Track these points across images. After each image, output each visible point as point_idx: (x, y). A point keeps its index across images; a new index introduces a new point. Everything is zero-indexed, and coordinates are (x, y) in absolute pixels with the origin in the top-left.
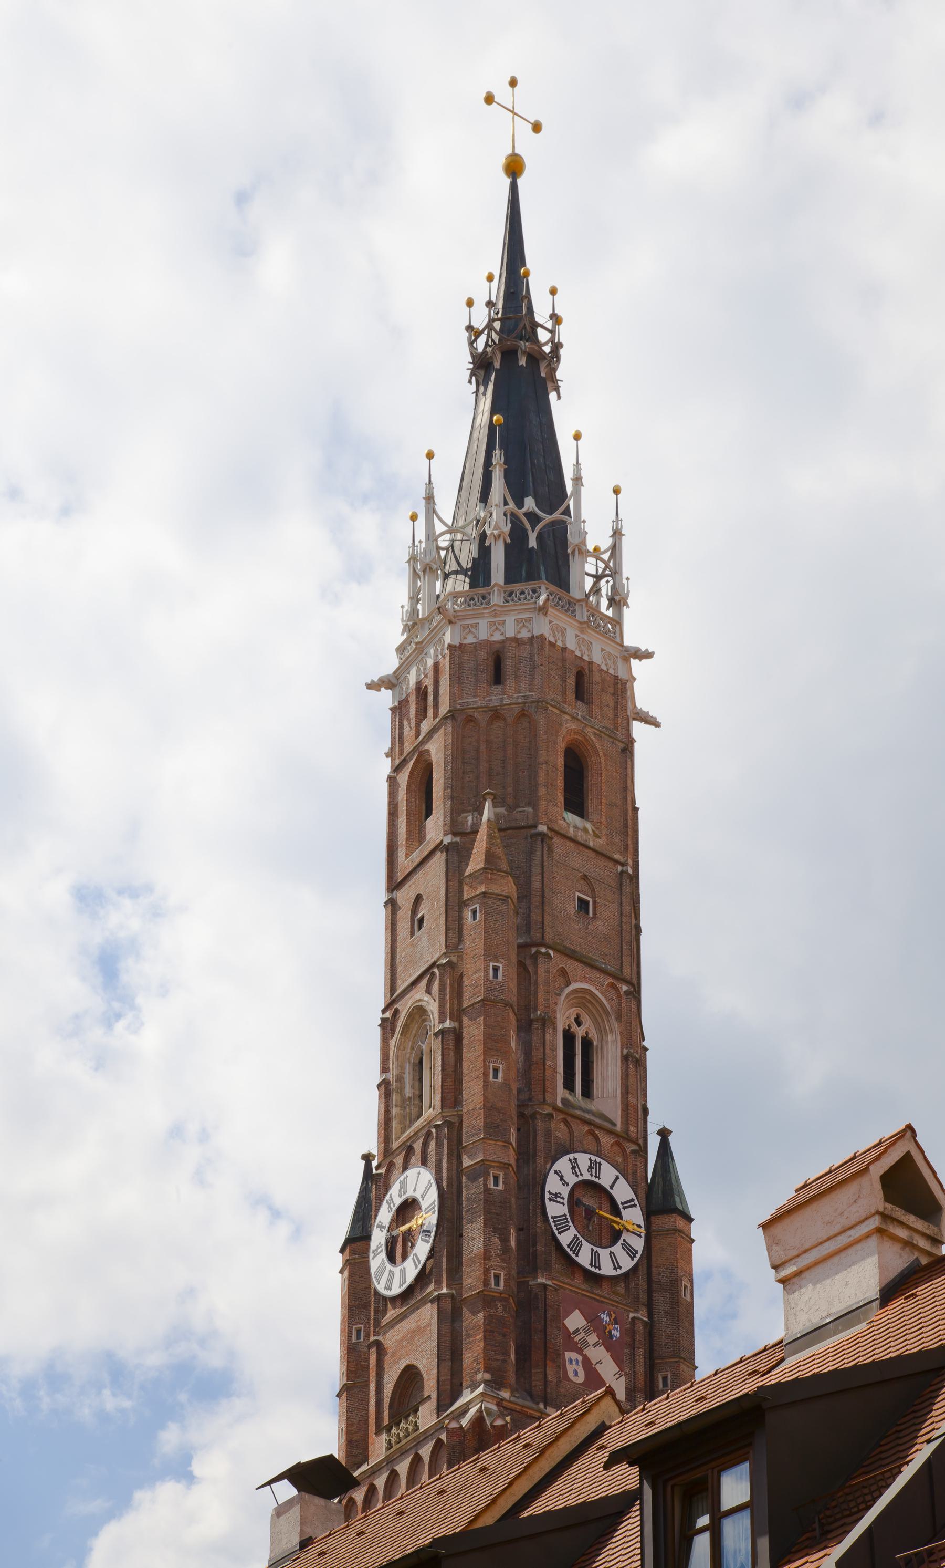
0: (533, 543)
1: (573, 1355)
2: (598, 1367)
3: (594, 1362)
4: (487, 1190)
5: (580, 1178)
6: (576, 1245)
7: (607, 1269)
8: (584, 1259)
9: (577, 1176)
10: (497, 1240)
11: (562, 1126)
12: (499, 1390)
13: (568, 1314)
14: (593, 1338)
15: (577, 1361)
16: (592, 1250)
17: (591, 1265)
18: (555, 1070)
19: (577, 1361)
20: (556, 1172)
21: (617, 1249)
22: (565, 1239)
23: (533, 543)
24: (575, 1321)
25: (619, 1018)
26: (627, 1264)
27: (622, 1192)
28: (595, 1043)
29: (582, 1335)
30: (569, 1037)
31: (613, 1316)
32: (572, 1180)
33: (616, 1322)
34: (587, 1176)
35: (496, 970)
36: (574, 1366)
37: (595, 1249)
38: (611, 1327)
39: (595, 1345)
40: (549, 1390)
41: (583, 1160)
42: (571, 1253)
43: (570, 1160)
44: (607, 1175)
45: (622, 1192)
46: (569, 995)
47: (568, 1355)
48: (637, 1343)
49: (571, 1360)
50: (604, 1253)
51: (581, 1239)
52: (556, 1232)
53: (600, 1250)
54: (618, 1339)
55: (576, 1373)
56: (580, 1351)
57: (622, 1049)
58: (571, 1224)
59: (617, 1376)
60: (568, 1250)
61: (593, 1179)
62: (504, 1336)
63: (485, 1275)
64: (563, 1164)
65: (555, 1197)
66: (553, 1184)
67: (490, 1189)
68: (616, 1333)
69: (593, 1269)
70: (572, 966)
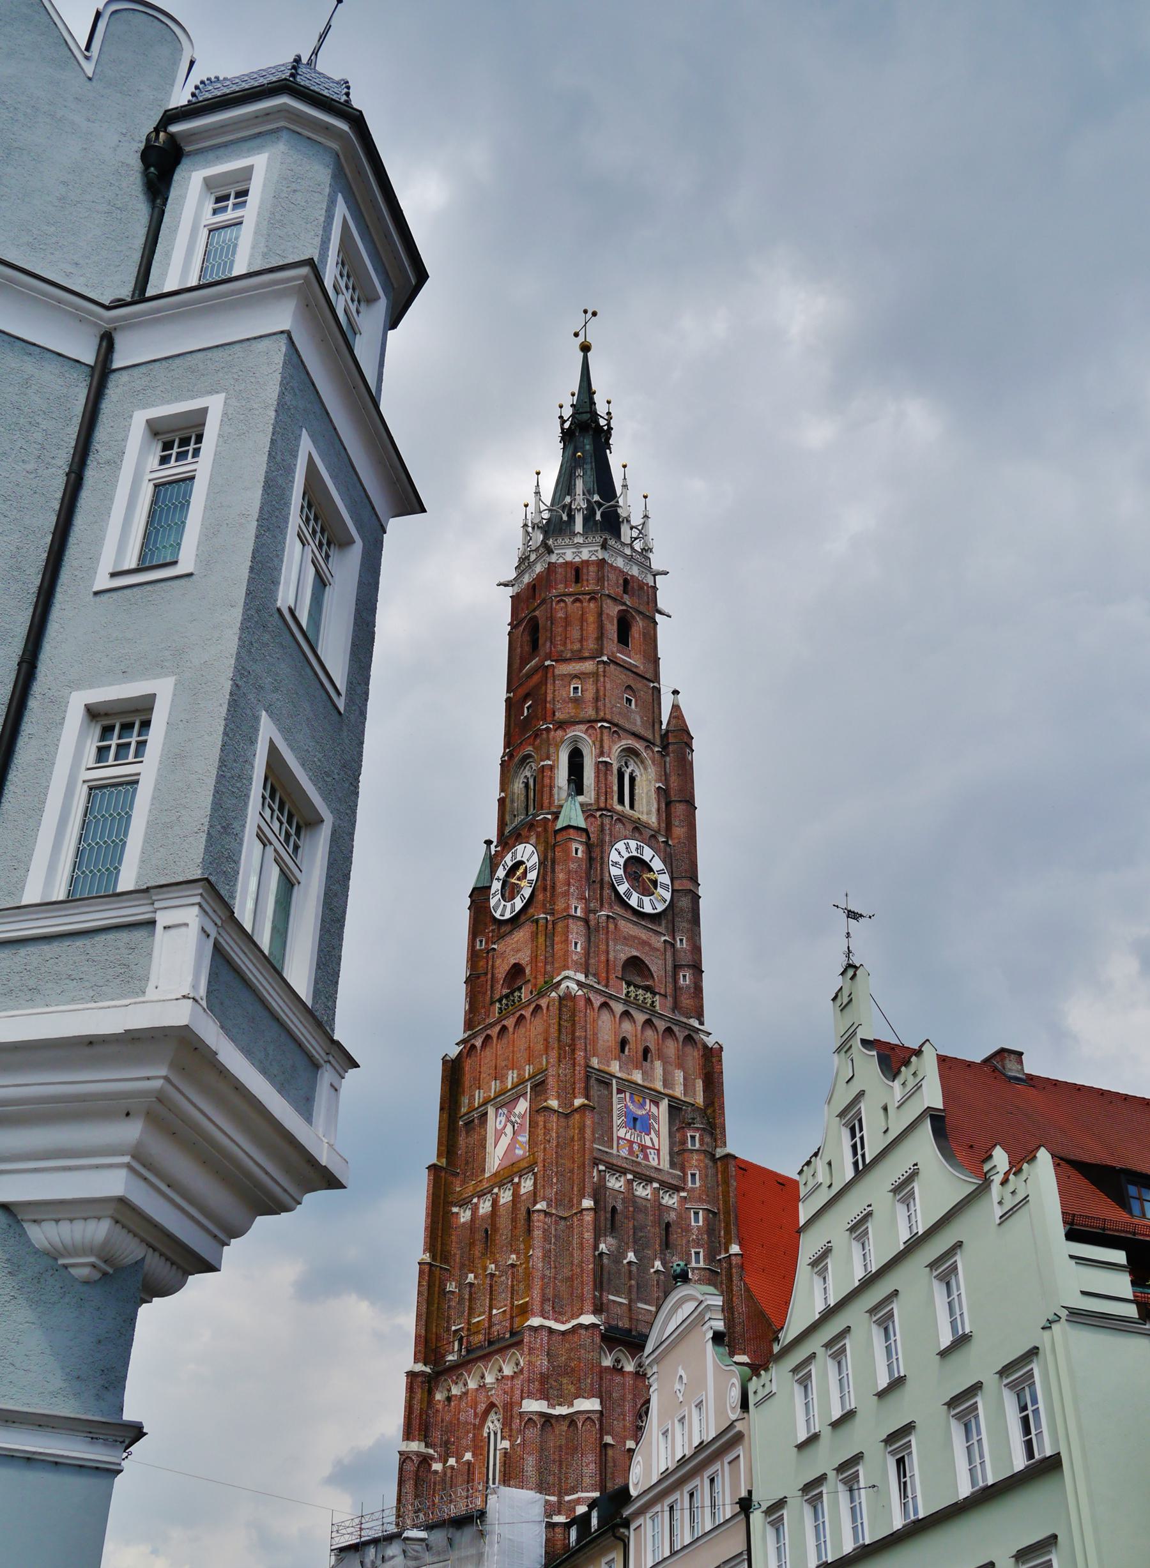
0: (598, 517)
6: (628, 893)
7: (648, 909)
8: (633, 902)
22: (622, 889)
23: (598, 517)
26: (660, 908)
27: (657, 864)
32: (626, 855)
34: (635, 854)
41: (633, 844)
44: (648, 854)
45: (657, 864)
50: (646, 900)
64: (620, 845)
65: (615, 864)
66: (614, 856)
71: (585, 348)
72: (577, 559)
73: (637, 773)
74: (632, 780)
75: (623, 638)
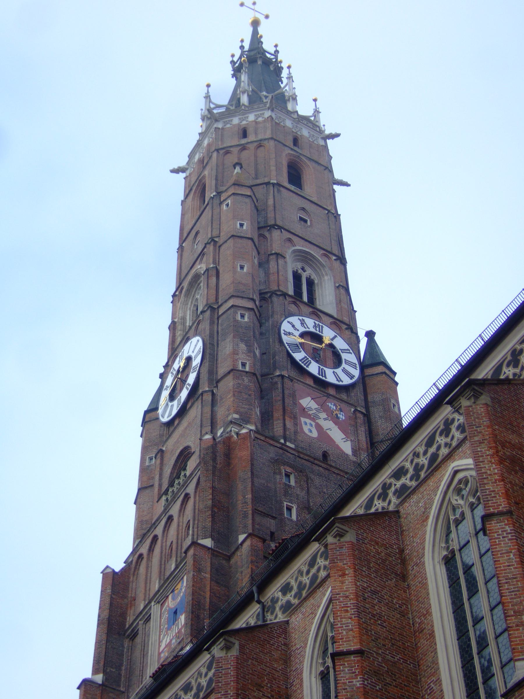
1: (308, 421)
2: (328, 431)
3: (325, 428)
4: (236, 321)
5: (307, 330)
7: (330, 378)
9: (305, 327)
10: (244, 346)
11: (293, 306)
12: (246, 424)
13: (302, 398)
14: (323, 415)
15: (311, 425)
16: (319, 367)
17: (319, 374)
18: (286, 279)
19: (311, 425)
20: (288, 322)
21: (339, 371)
24: (307, 402)
25: (331, 269)
28: (316, 282)
29: (314, 411)
30: (297, 277)
31: (339, 407)
33: (341, 410)
34: (312, 330)
35: (242, 225)
36: (309, 427)
37: (322, 367)
38: (337, 412)
39: (325, 419)
40: (287, 433)
42: (303, 365)
43: (300, 320)
46: (294, 251)
47: (303, 420)
48: (358, 424)
49: (306, 424)
51: (310, 359)
52: (291, 352)
53: (325, 368)
54: (343, 420)
55: (311, 431)
56: (313, 420)
57: (335, 283)
58: (301, 350)
59: (345, 440)
60: (300, 363)
61: (318, 332)
62: (250, 395)
63: (233, 361)
67: (238, 321)
68: (342, 417)
69: (321, 377)
70: (295, 239)
71: (255, 24)
72: (244, 122)
73: (314, 276)
74: (310, 283)
75: (295, 176)
